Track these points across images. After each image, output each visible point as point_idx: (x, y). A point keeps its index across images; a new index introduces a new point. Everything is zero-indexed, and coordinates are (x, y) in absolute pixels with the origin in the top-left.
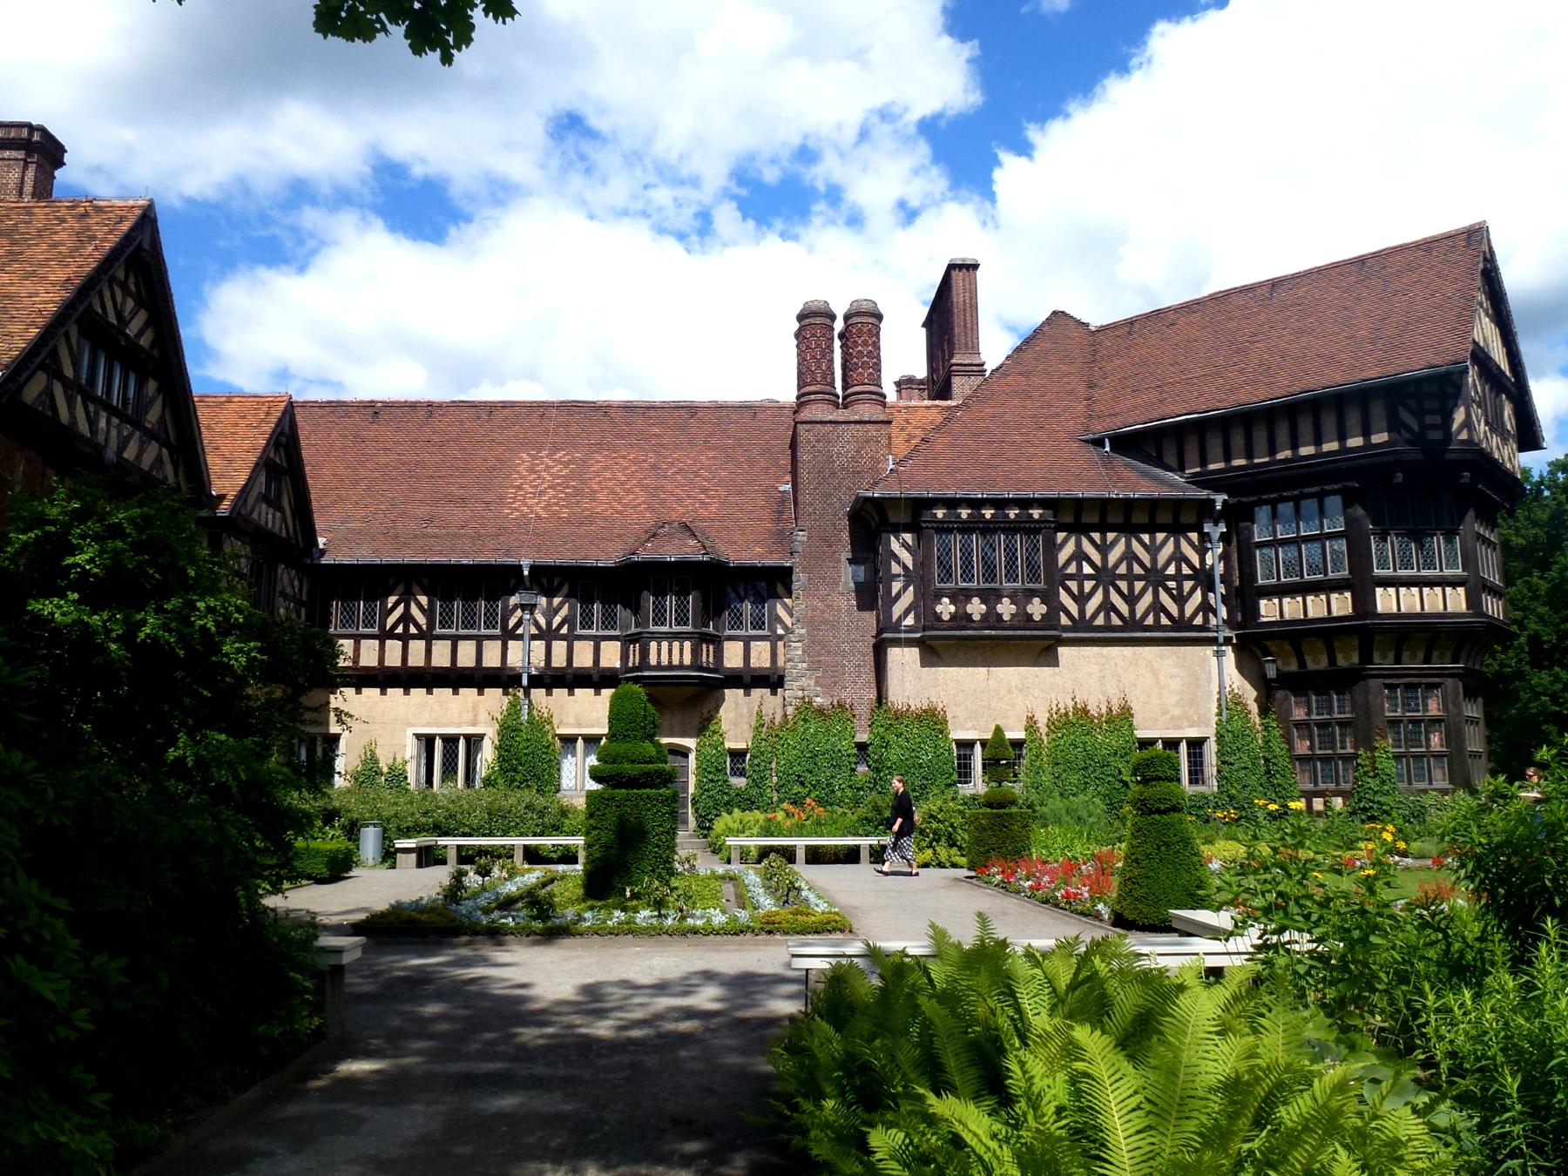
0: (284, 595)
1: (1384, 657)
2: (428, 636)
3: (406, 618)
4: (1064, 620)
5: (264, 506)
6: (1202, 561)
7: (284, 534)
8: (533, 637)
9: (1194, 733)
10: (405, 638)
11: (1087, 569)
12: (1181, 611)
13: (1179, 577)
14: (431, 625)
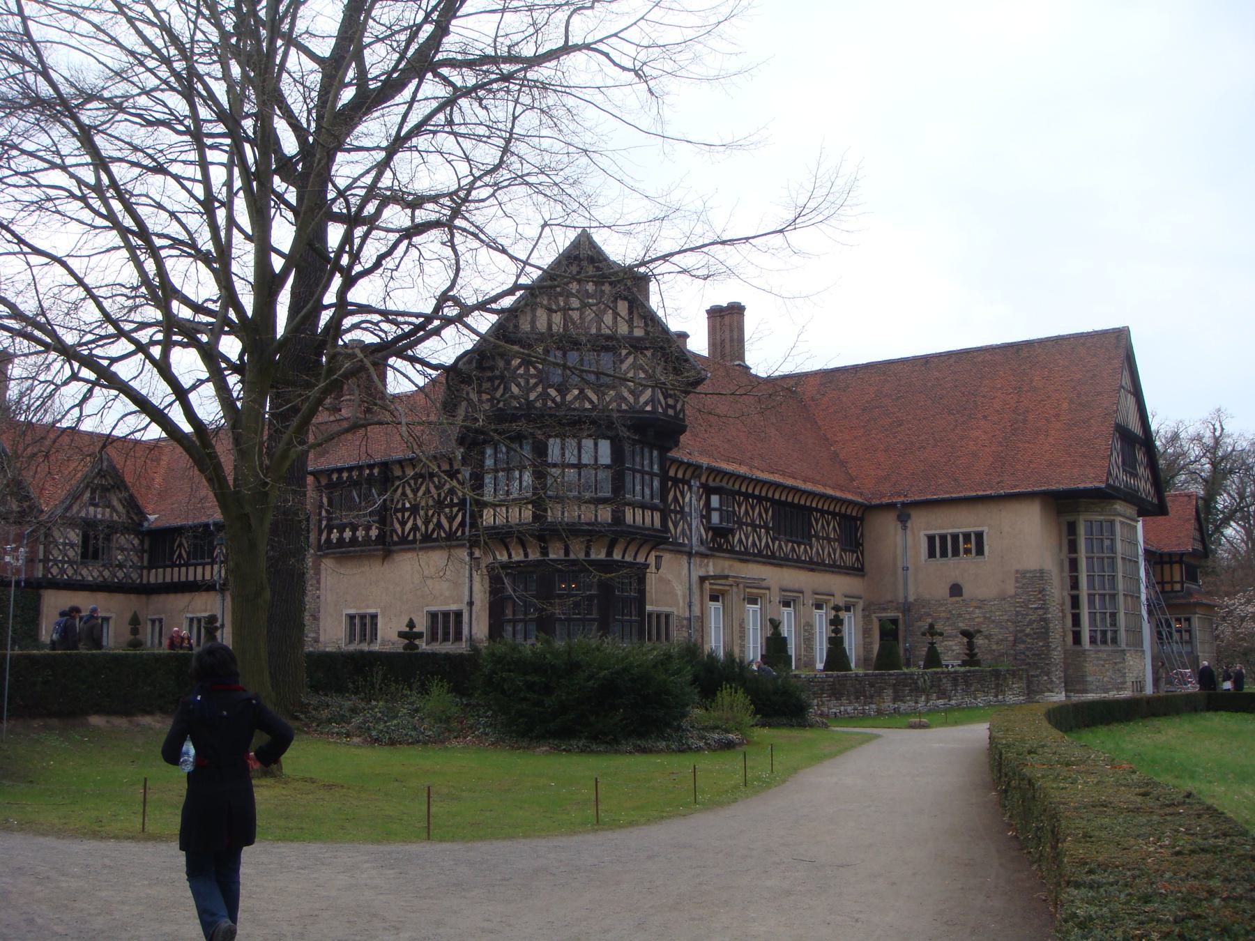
0: (122, 549)
1: (502, 555)
2: (187, 565)
3: (180, 556)
4: (395, 538)
5: (91, 509)
7: (115, 517)
9: (454, 607)
10: (180, 566)
14: (189, 559)
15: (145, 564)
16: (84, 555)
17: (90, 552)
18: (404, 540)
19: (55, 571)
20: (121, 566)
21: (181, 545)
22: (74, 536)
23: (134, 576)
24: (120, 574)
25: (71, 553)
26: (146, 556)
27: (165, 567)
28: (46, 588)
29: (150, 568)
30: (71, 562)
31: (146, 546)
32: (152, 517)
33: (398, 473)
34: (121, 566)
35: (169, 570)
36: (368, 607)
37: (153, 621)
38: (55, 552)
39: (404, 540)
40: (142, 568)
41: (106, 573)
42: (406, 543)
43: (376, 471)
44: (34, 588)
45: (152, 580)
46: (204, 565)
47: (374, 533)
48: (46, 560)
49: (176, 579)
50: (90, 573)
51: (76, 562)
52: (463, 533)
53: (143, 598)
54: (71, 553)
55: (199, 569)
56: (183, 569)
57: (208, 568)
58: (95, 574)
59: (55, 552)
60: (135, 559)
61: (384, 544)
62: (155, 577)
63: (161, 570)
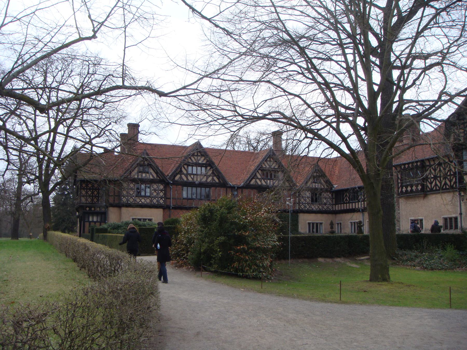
2: (349, 203)
3: (346, 199)
4: (428, 189)
6: (455, 170)
8: (362, 201)
10: (346, 203)
11: (432, 176)
12: (451, 184)
13: (450, 175)
15: (334, 203)
16: (312, 200)
17: (315, 199)
18: (432, 190)
19: (302, 207)
20: (325, 204)
21: (346, 196)
22: (308, 194)
23: (330, 207)
24: (325, 207)
25: (308, 200)
26: (334, 200)
27: (341, 204)
28: (300, 213)
29: (336, 204)
30: (308, 204)
31: (334, 196)
32: (335, 186)
33: (428, 164)
34: (325, 204)
35: (342, 205)
36: (419, 216)
37: (338, 224)
38: (302, 200)
39: (432, 190)
40: (333, 205)
41: (320, 207)
42: (433, 191)
43: (419, 164)
44: (296, 213)
45: (337, 209)
46: (355, 203)
47: (420, 187)
48: (299, 203)
49: (345, 208)
50: (315, 207)
51: (309, 203)
52: (456, 186)
53: (334, 215)
54: (308, 200)
55: (354, 204)
56: (348, 204)
57: (357, 204)
58: (317, 207)
59: (302, 200)
60: (330, 201)
61: (424, 191)
62: (338, 208)
63: (340, 205)
